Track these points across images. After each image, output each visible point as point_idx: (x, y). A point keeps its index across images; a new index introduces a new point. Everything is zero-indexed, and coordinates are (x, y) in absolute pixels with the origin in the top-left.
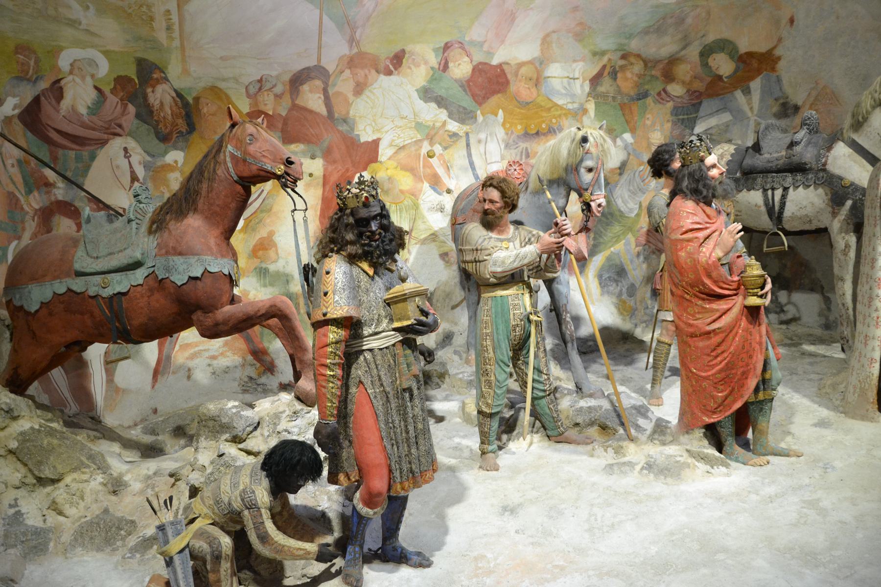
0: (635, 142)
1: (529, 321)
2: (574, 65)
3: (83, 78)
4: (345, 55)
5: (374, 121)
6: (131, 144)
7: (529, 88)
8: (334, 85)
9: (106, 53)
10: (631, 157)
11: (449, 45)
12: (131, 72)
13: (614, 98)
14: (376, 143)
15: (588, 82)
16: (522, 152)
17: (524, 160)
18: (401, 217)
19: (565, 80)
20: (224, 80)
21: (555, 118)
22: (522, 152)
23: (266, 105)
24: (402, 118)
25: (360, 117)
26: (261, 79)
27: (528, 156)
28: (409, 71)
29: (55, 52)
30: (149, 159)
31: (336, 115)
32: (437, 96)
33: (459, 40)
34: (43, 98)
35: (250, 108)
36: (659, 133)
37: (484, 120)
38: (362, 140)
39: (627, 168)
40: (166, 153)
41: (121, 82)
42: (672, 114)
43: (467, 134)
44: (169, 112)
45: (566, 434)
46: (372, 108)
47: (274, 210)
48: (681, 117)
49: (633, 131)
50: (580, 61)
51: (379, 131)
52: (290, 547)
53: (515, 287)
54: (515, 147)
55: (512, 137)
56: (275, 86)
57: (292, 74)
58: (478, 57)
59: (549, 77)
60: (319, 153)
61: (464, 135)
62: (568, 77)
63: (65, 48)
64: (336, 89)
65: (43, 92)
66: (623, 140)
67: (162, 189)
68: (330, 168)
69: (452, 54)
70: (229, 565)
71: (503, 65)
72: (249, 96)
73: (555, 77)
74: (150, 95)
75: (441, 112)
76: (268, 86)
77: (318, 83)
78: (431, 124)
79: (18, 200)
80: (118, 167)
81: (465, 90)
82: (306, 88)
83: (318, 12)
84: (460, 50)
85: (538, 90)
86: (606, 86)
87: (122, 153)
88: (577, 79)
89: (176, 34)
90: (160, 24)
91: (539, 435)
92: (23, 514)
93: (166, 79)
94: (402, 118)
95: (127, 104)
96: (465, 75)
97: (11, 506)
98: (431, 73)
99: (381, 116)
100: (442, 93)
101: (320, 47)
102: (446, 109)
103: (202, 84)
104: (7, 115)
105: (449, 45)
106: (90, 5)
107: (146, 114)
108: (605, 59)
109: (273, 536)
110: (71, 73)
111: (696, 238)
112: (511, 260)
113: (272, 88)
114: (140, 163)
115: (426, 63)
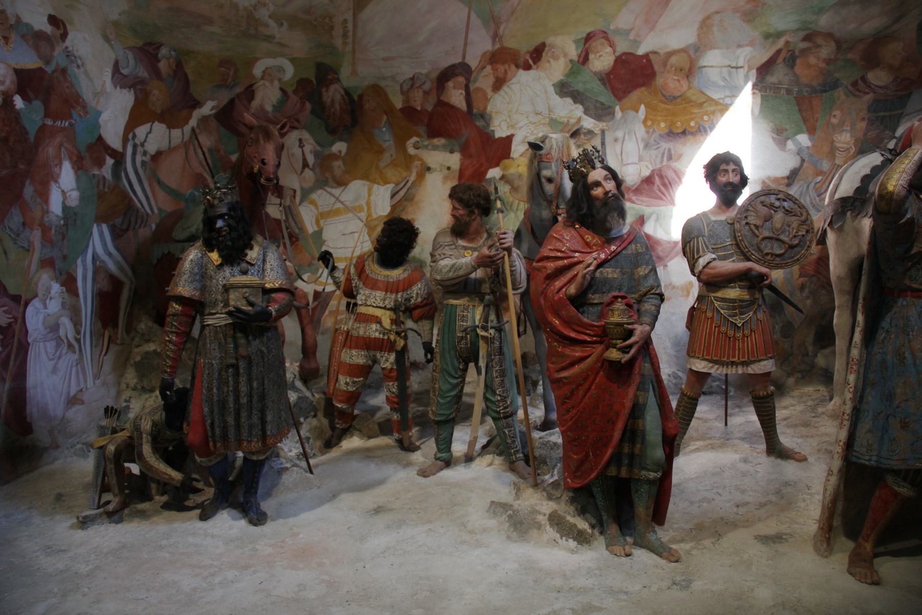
0: (813, 146)
1: (477, 335)
2: (739, 51)
3: (272, 82)
4: (488, 51)
5: (509, 117)
6: (306, 135)
7: (678, 81)
8: (475, 81)
9: (293, 60)
10: (805, 165)
11: (592, 35)
12: (311, 74)
13: (789, 92)
14: (509, 139)
15: (754, 72)
16: (663, 154)
17: (665, 163)
19: (725, 70)
20: (384, 78)
21: (707, 115)
22: (663, 154)
23: (416, 101)
24: (537, 114)
25: (496, 113)
26: (414, 76)
27: (670, 158)
28: (547, 64)
29: (251, 63)
30: (318, 148)
31: (475, 111)
32: (573, 91)
33: (604, 29)
34: (237, 101)
35: (403, 105)
36: (848, 135)
37: (623, 117)
38: (497, 135)
39: (798, 177)
40: (333, 144)
41: (302, 84)
42: (869, 110)
43: (603, 132)
44: (338, 108)
45: (516, 463)
46: (508, 104)
47: (416, 199)
48: (882, 114)
49: (811, 131)
50: (747, 45)
51: (513, 127)
52: (158, 469)
53: (467, 299)
54: (656, 147)
55: (653, 136)
56: (424, 83)
57: (439, 71)
58: (622, 47)
59: (705, 67)
60: (457, 148)
61: (600, 132)
62: (729, 66)
63: (261, 58)
64: (477, 85)
65: (238, 96)
66: (797, 143)
67: (327, 175)
69: (594, 44)
70: (112, 466)
71: (650, 55)
72: (402, 93)
73: (712, 67)
74: (324, 93)
75: (577, 108)
76: (418, 84)
77: (461, 79)
78: (566, 120)
79: (205, 179)
80: (293, 155)
81: (604, 84)
82: (450, 84)
83: (466, 10)
84: (603, 40)
85: (690, 82)
86: (779, 75)
87: (297, 143)
88: (741, 67)
89: (350, 40)
90: (338, 32)
91: (502, 458)
92: (129, 408)
93: (338, 80)
94: (537, 114)
95: (305, 102)
96: (606, 68)
97: (126, 401)
98: (570, 65)
99: (516, 112)
100: (580, 87)
101: (466, 44)
102: (582, 104)
103: (366, 83)
104: (205, 115)
105: (592, 35)
106: (284, 21)
107: (320, 110)
108: (781, 43)
109: (146, 457)
110: (262, 78)
111: (545, 267)
112: (448, 269)
113: (422, 85)
114: (311, 152)
115: (565, 55)
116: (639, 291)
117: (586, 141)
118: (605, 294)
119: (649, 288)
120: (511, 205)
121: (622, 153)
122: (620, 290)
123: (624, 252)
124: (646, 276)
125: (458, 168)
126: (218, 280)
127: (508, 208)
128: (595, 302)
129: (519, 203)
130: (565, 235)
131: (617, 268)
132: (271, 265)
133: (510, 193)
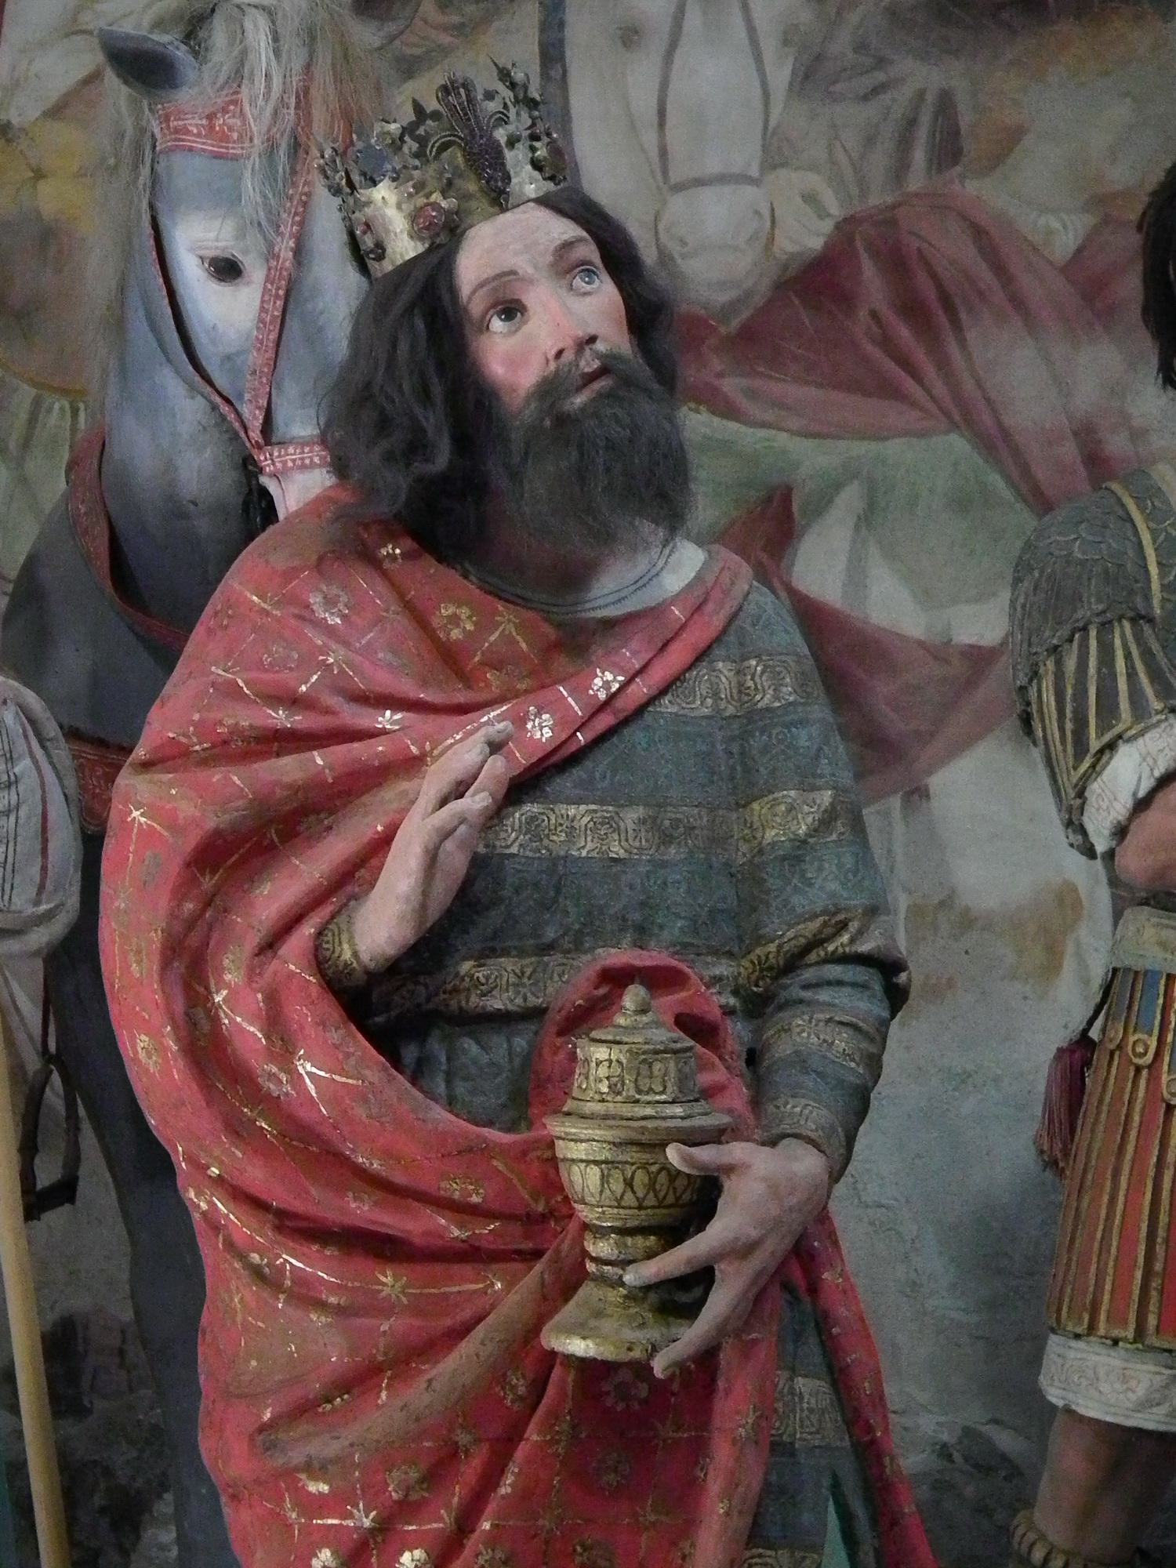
16: (912, 123)
17: (916, 181)
22: (912, 123)
54: (867, 82)
116: (760, 940)
117: (446, 39)
118: (554, 960)
119: (814, 925)
121: (662, 113)
122: (642, 934)
123: (668, 706)
124: (798, 853)
128: (496, 1003)
129: (37, 403)
130: (315, 600)
131: (631, 802)
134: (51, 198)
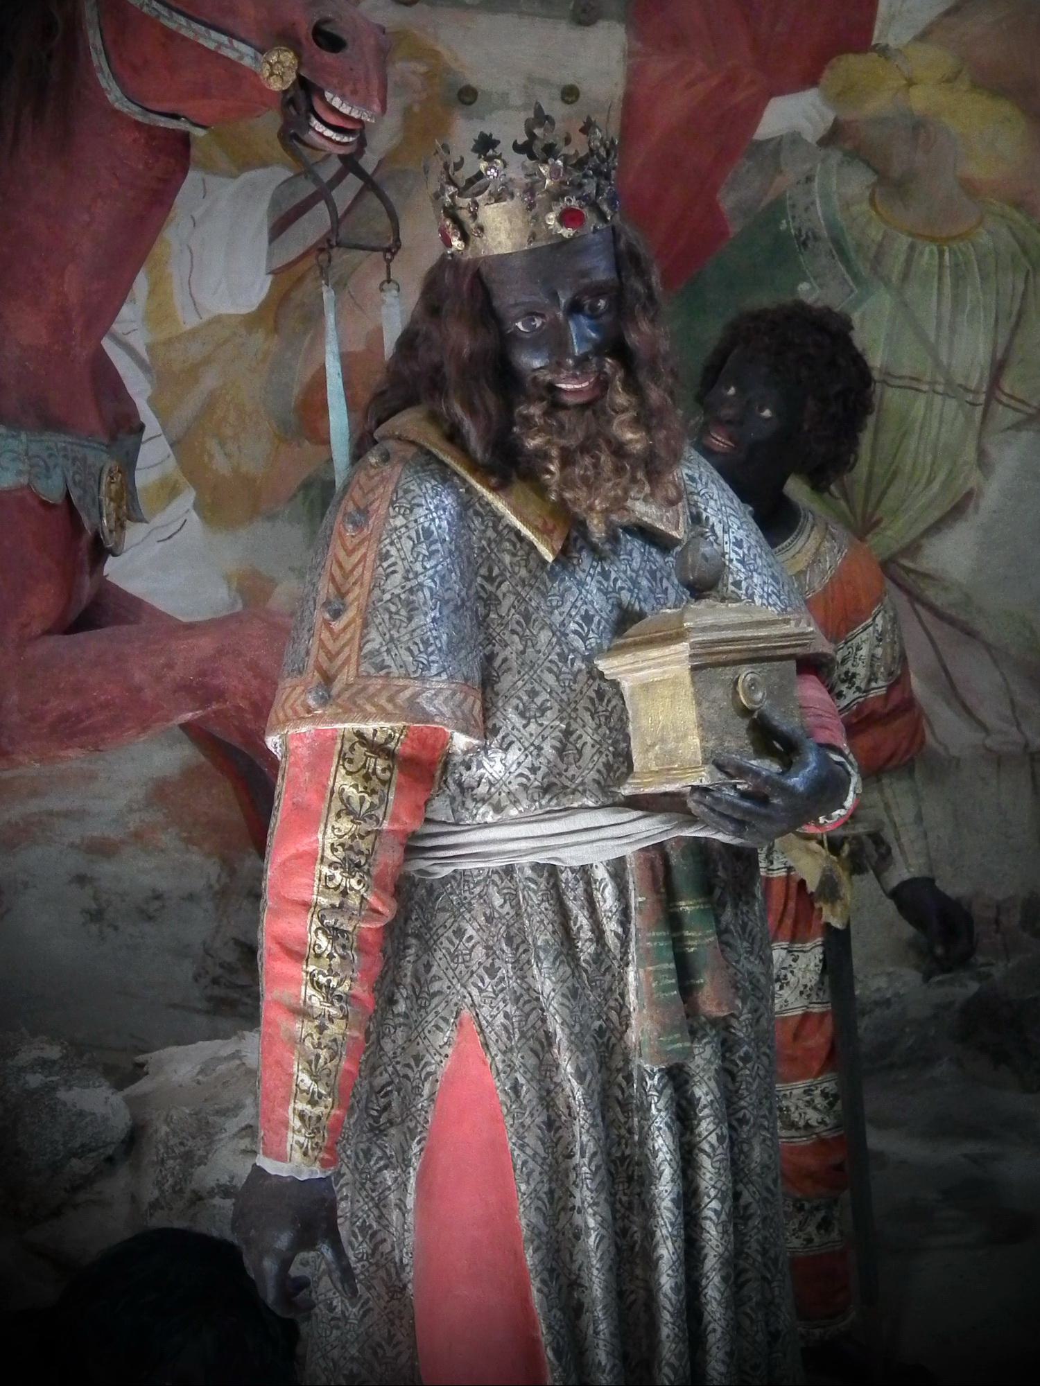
18: (957, 300)
68: (658, 67)
120: (877, 260)
125: (619, 92)
126: (560, 633)
127: (864, 268)
129: (912, 247)
132: (739, 544)
133: (872, 201)
134: (919, 100)
